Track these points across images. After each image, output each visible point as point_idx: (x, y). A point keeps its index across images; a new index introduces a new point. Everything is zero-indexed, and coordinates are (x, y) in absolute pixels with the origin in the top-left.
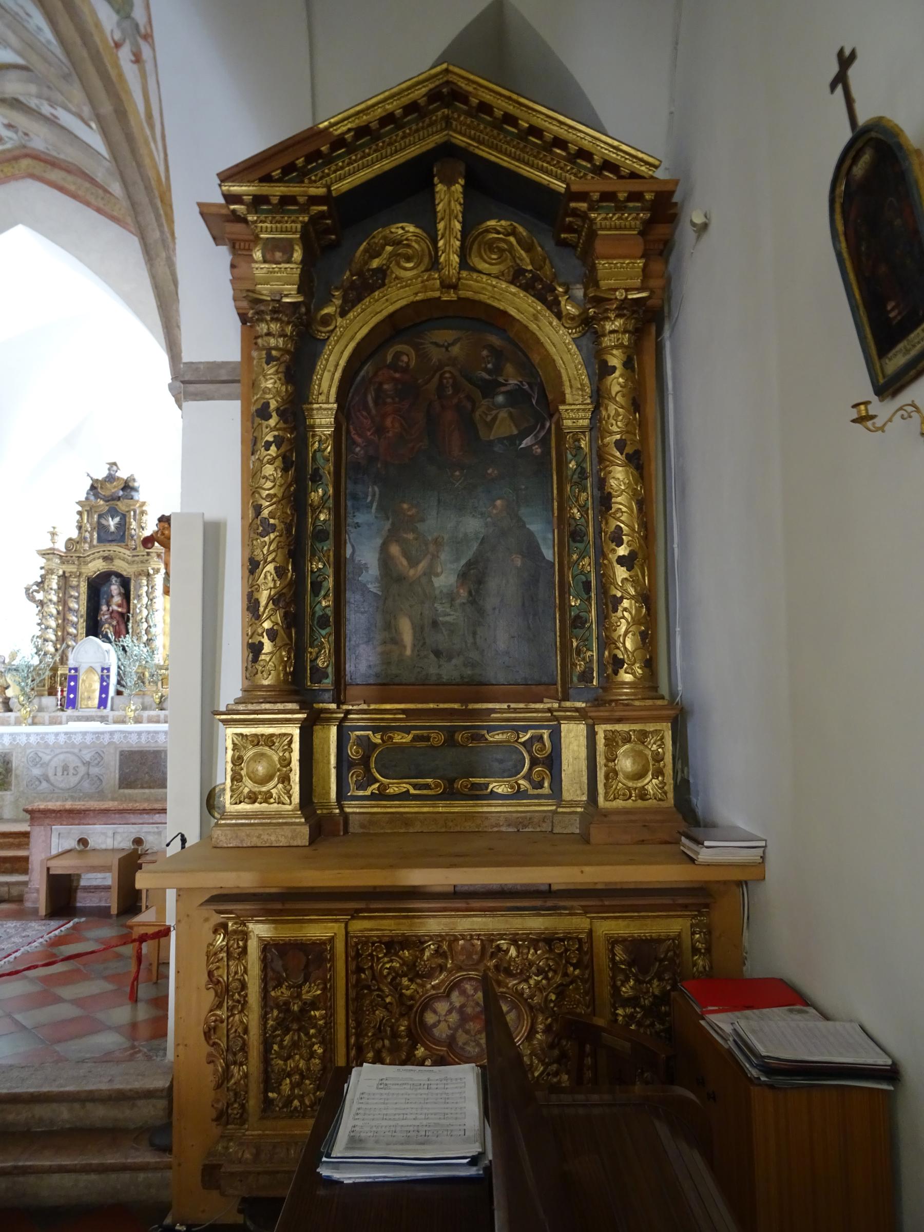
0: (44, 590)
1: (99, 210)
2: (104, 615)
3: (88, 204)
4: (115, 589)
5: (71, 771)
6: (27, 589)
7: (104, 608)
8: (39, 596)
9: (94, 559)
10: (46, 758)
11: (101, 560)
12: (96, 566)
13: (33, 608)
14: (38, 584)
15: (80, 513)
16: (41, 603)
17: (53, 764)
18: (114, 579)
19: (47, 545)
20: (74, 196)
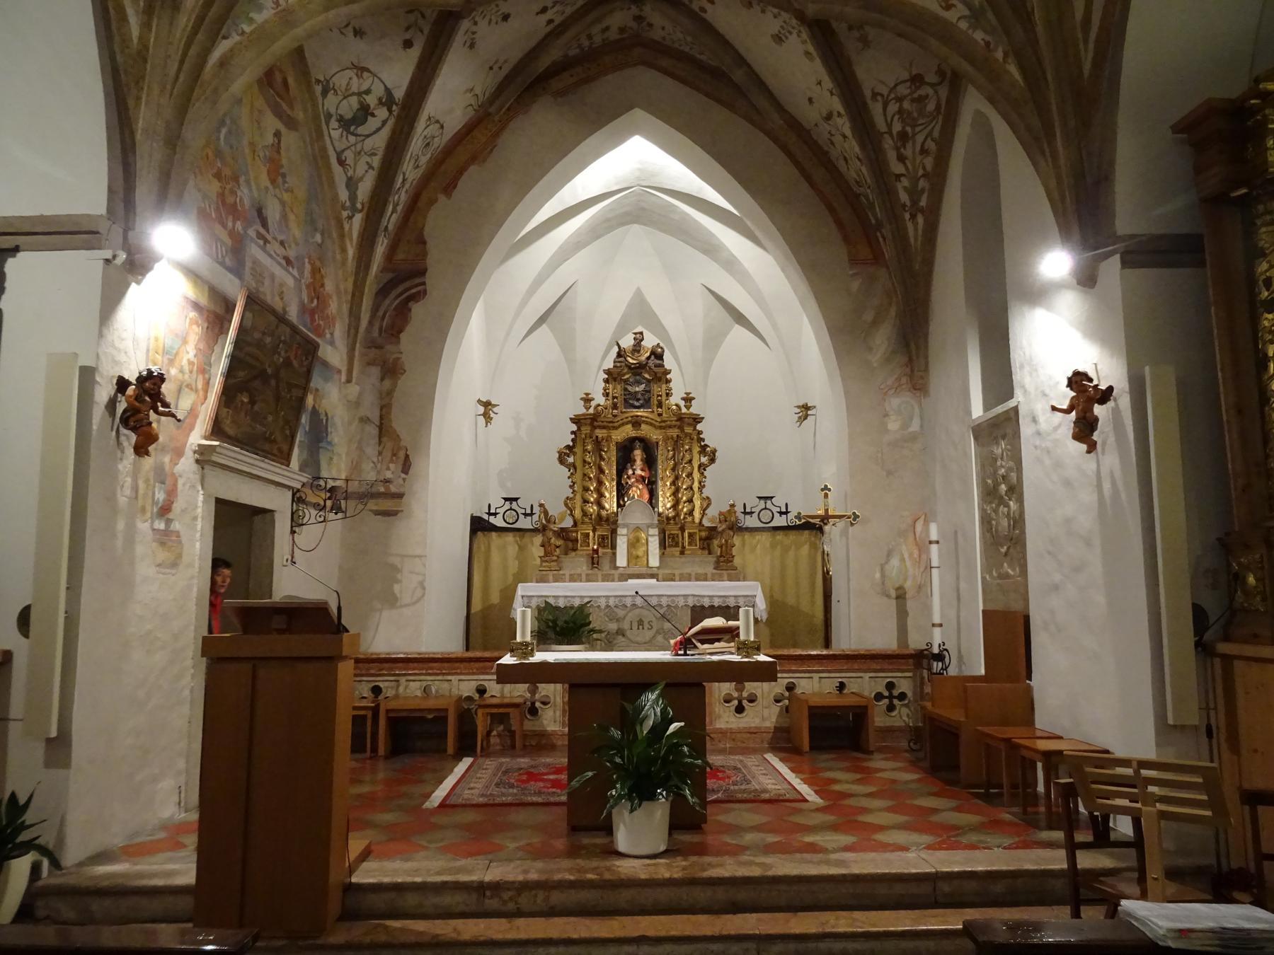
0: (575, 454)
1: (707, 95)
2: (629, 478)
3: (697, 89)
4: (638, 454)
5: (646, 626)
6: (560, 453)
7: (630, 472)
8: (571, 460)
9: (623, 424)
10: (621, 613)
11: (629, 426)
12: (628, 431)
13: (565, 472)
14: (568, 447)
15: (606, 381)
16: (569, 466)
17: (628, 619)
18: (638, 444)
19: (582, 411)
20: (683, 81)
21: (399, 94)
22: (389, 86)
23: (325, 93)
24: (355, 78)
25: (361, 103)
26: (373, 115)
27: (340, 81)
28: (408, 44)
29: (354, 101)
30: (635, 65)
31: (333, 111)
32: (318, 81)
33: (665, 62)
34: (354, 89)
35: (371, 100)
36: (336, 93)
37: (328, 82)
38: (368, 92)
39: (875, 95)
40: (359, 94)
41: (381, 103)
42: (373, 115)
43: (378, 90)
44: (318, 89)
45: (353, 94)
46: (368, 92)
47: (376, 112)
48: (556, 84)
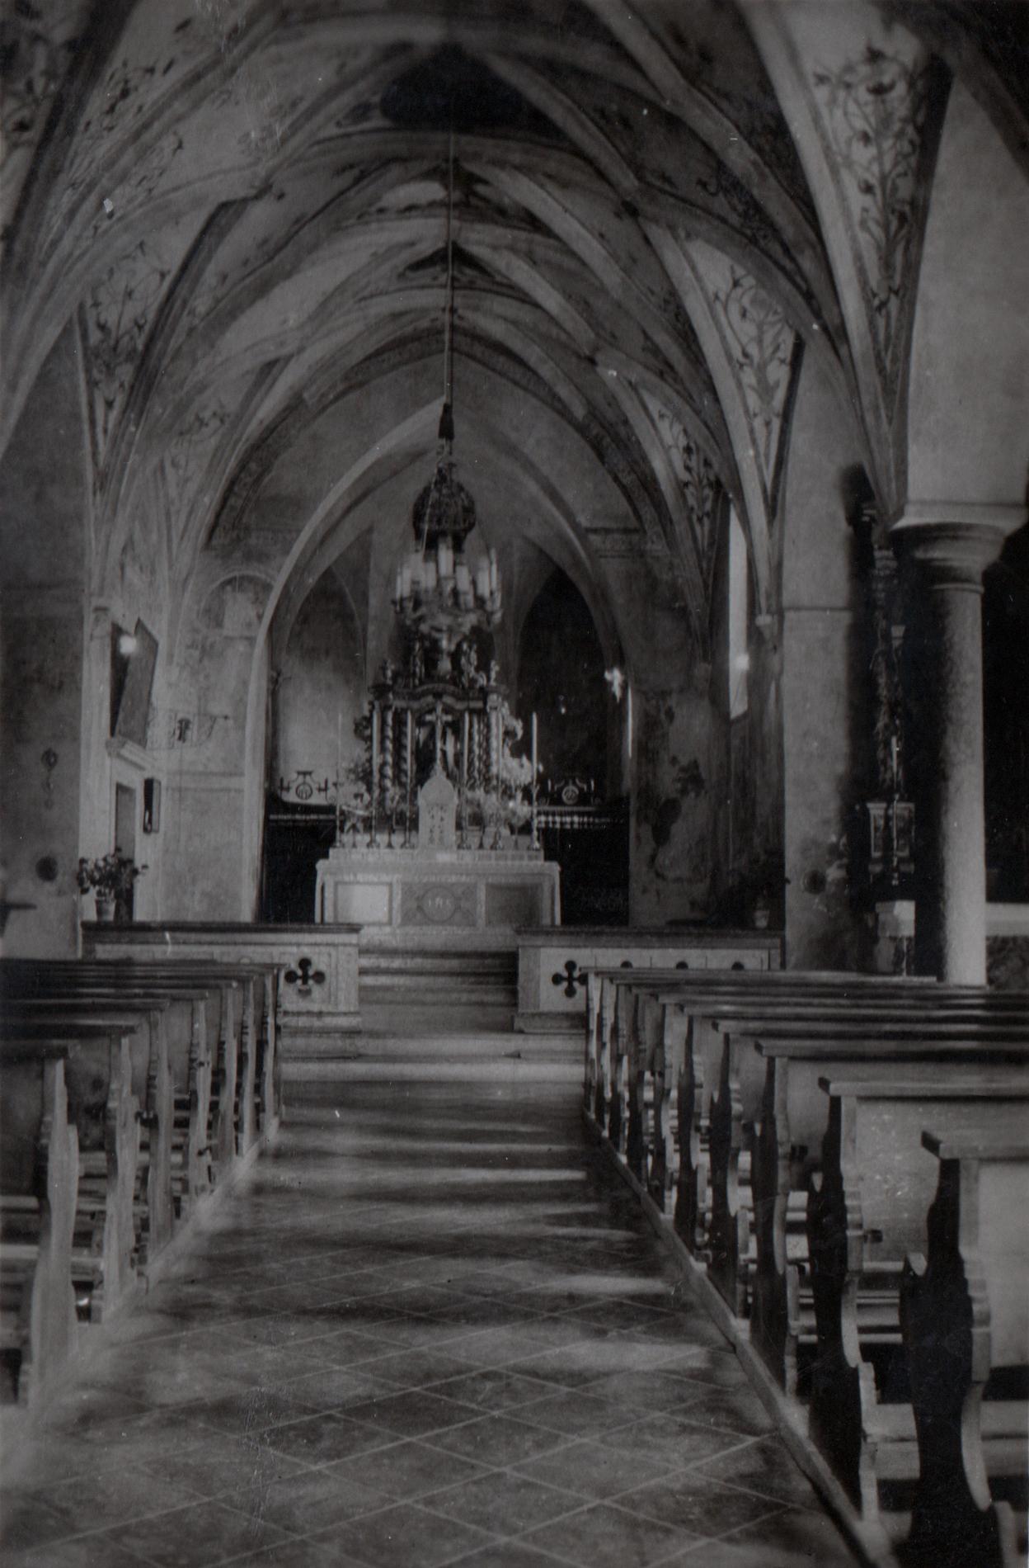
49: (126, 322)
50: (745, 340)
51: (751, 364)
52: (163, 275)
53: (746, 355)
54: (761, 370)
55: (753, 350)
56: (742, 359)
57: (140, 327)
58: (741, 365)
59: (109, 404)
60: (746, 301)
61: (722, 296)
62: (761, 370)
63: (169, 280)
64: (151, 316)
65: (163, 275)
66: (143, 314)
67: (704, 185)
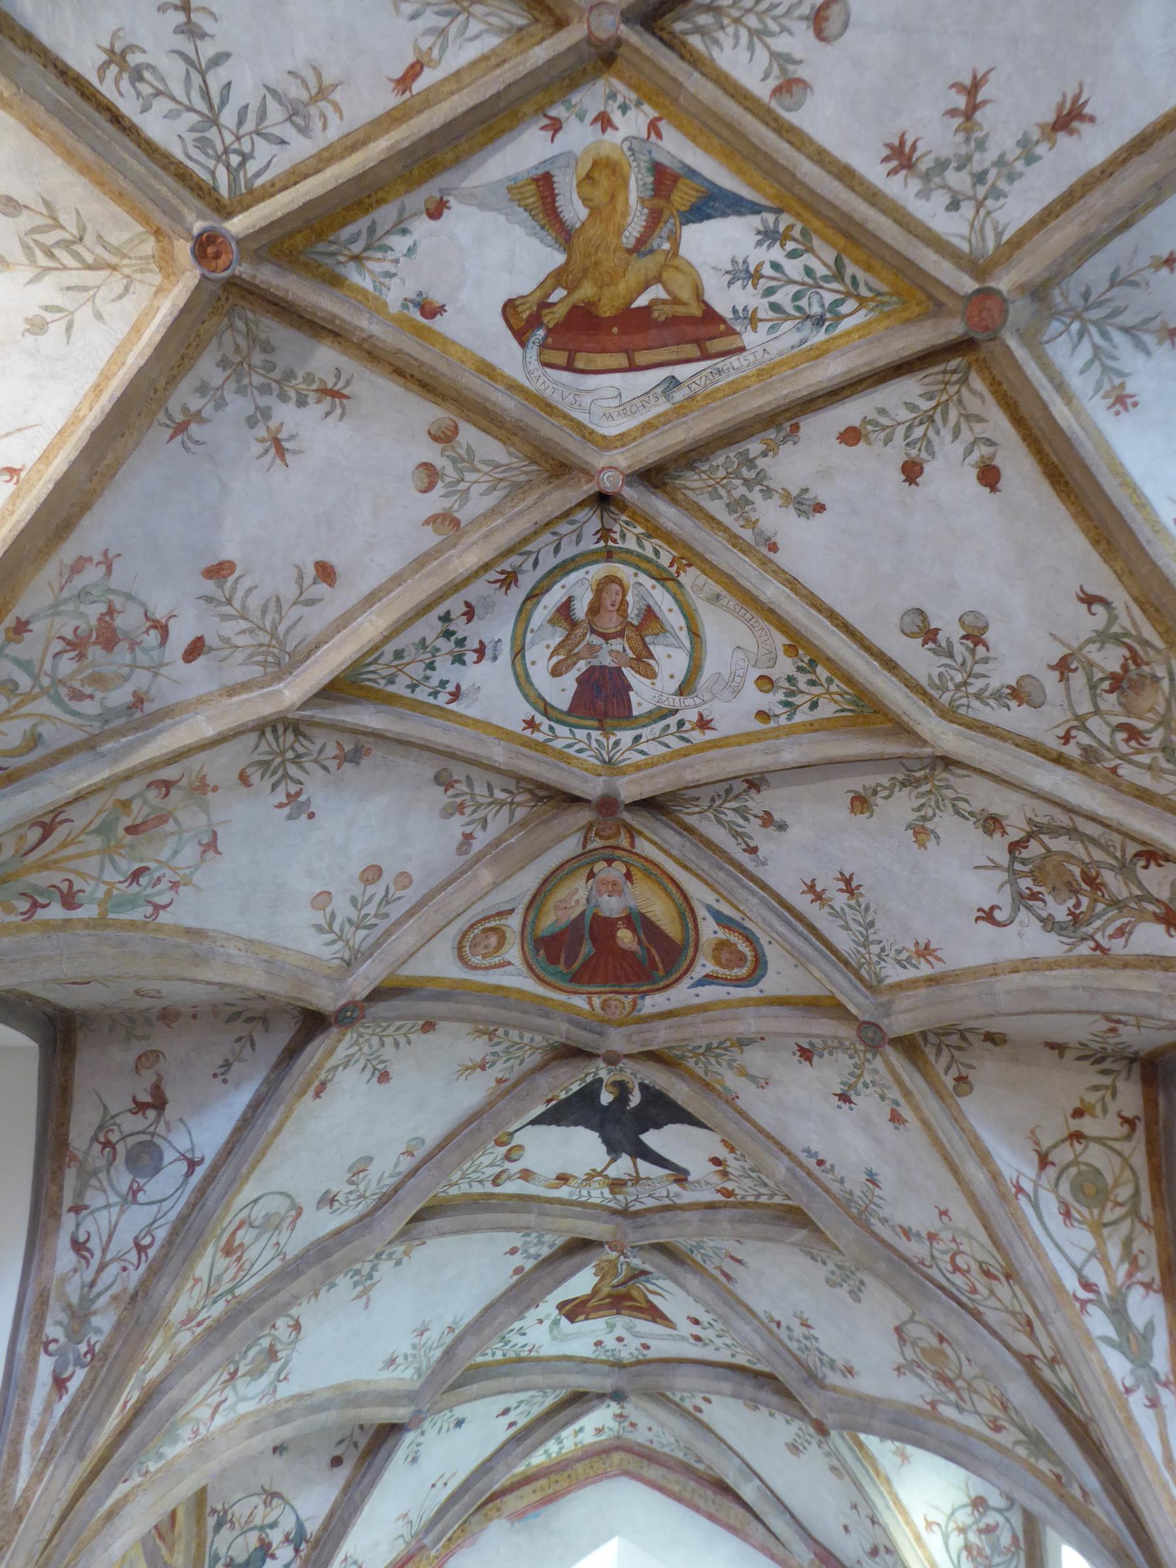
1: (711, 1517)
3: (697, 1510)
20: (679, 1499)
21: (312, 1528)
22: (302, 1516)
23: (219, 1526)
24: (261, 1507)
25: (261, 1540)
26: (273, 1557)
27: (241, 1511)
28: (337, 1462)
29: (253, 1539)
30: (615, 1476)
31: (222, 1552)
32: (214, 1511)
33: (654, 1472)
34: (258, 1521)
35: (276, 1536)
36: (233, 1527)
37: (226, 1512)
38: (273, 1525)
39: (929, 1525)
40: (262, 1528)
41: (287, 1539)
42: (273, 1557)
43: (288, 1524)
44: (211, 1521)
45: (254, 1528)
46: (273, 1525)
47: (278, 1553)
48: (512, 1502)
49: (124, 1240)
50: (1078, 1257)
51: (1098, 1303)
52: (192, 1165)
53: (1087, 1286)
54: (1117, 1312)
55: (1095, 1273)
56: (1082, 1294)
57: (141, 1249)
58: (1084, 1303)
59: (60, 1383)
60: (1065, 1188)
61: (1027, 1186)
62: (1117, 1312)
63: (200, 1171)
64: (161, 1234)
65: (192, 1165)
66: (149, 1229)
67: (988, 916)
